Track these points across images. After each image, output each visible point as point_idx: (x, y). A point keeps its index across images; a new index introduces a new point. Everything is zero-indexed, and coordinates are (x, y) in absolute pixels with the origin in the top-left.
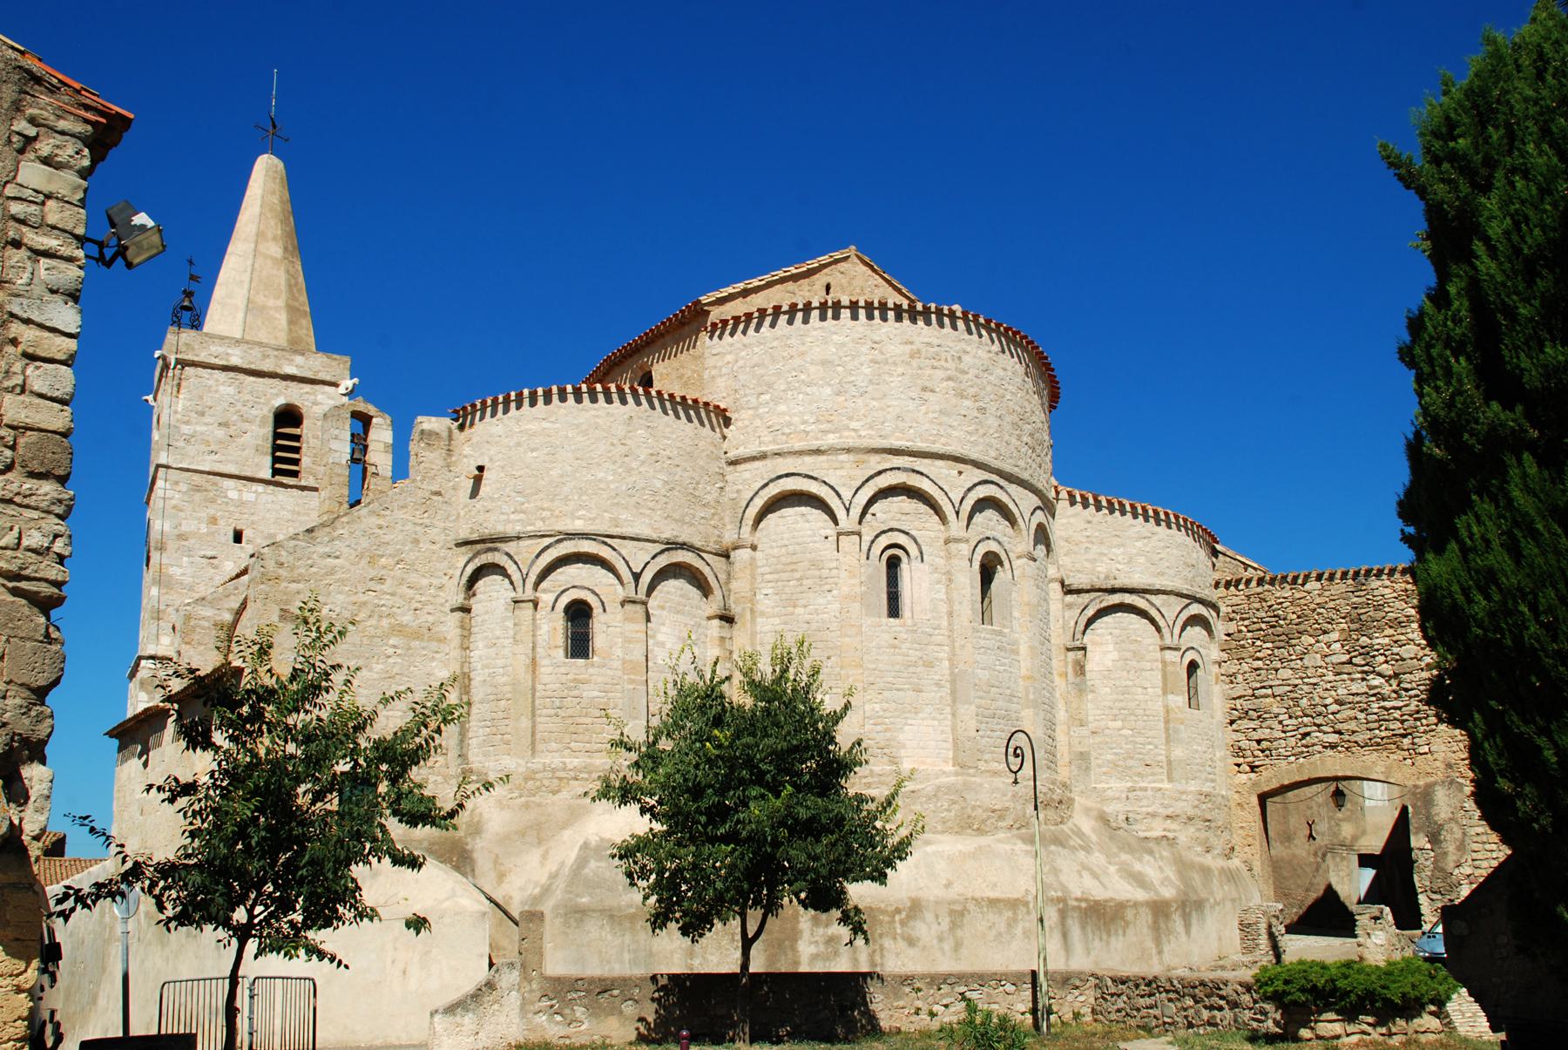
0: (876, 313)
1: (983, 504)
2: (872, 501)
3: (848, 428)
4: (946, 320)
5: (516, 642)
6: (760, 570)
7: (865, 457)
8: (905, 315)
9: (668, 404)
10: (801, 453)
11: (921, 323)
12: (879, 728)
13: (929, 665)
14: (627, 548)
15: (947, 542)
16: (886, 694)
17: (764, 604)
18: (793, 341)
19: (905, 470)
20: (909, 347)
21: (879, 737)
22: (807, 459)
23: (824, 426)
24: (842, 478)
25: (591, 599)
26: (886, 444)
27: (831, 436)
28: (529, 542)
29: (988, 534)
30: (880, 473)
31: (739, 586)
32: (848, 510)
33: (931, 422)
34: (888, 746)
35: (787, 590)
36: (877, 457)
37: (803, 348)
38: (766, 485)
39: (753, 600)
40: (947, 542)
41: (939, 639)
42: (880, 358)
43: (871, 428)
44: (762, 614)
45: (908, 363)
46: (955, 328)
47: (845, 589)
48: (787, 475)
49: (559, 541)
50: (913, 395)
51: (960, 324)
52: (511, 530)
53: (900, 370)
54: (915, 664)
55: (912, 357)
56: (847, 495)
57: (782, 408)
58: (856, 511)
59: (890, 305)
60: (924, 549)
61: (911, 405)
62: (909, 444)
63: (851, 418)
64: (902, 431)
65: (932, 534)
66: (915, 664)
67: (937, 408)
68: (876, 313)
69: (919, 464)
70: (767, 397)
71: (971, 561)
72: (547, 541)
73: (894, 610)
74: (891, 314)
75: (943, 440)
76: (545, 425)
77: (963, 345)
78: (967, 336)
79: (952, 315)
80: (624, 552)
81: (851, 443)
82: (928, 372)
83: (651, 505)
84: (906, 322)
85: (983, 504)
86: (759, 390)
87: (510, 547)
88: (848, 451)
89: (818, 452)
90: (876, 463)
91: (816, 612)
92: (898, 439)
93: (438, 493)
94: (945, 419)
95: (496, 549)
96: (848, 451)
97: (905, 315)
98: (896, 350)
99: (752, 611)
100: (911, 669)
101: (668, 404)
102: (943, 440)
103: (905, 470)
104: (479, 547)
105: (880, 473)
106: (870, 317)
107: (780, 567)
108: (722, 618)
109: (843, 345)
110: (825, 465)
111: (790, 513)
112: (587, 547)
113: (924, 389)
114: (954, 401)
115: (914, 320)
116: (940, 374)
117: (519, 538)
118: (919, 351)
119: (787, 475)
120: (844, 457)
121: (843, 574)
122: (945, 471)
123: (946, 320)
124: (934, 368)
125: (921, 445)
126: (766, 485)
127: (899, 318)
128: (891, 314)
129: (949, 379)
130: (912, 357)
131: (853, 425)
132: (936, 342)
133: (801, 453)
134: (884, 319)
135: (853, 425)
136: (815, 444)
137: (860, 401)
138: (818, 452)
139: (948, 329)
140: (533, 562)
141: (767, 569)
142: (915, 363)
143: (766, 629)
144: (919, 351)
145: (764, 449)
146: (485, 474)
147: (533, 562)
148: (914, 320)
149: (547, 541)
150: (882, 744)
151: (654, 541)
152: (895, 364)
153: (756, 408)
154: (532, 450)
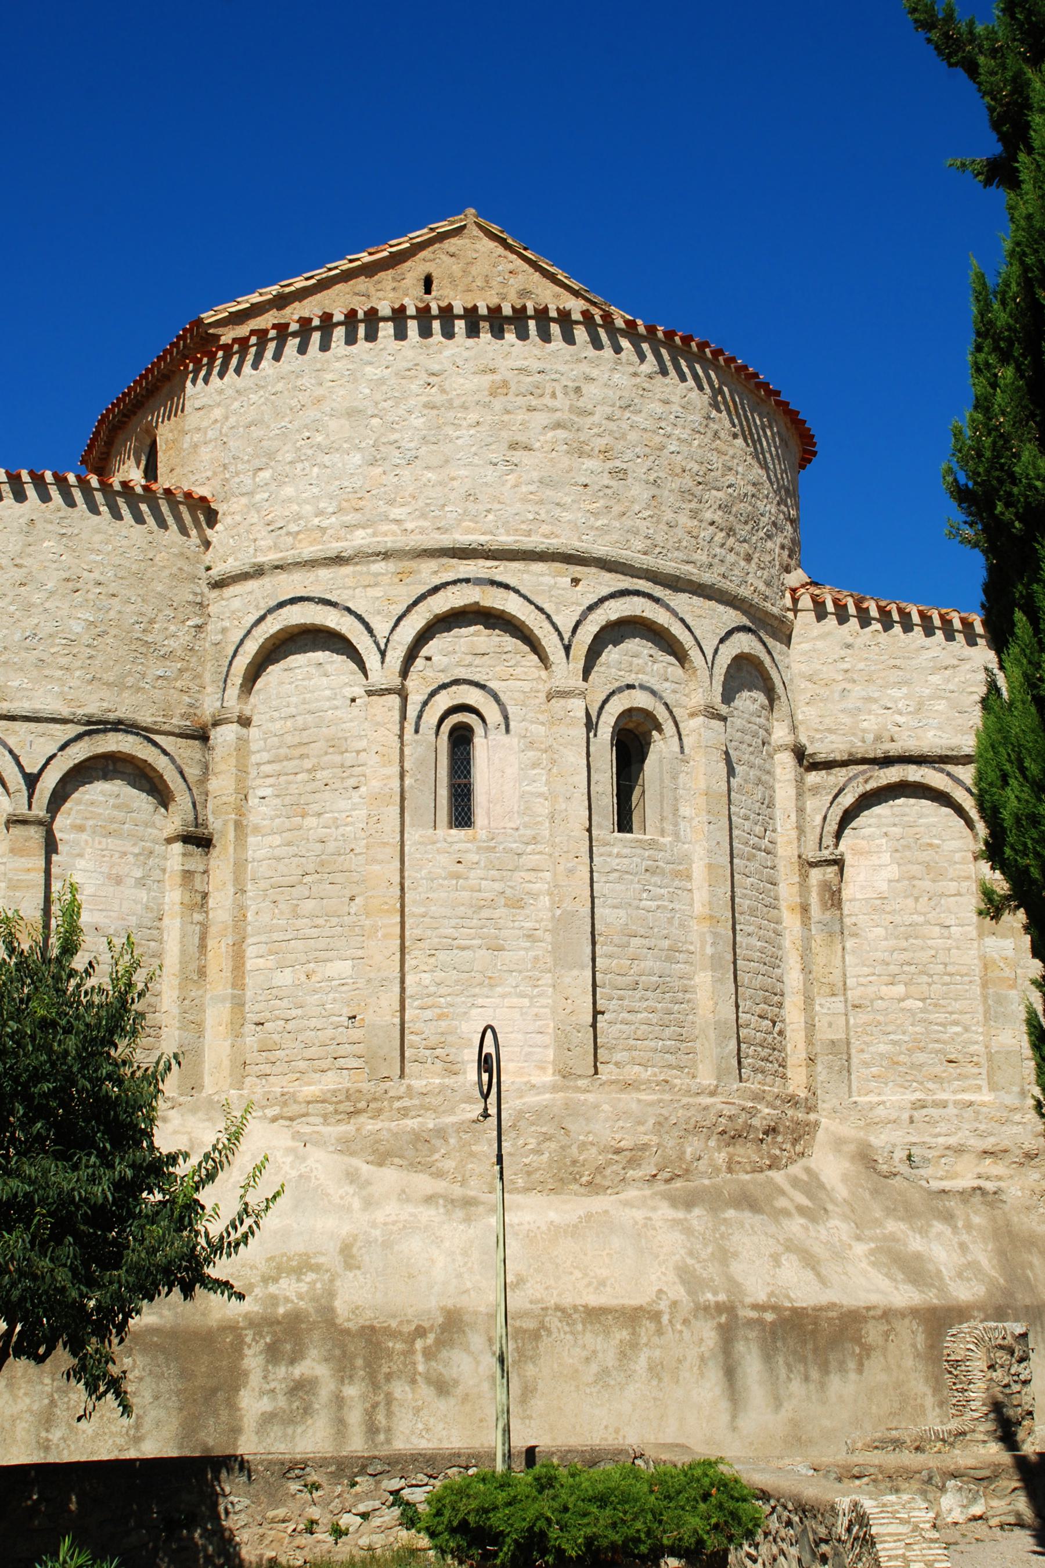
0: (436, 325)
1: (615, 632)
2: (424, 637)
3: (386, 519)
4: (555, 329)
6: (254, 759)
7: (413, 564)
8: (484, 325)
11: (510, 337)
12: (428, 1014)
13: (516, 904)
15: (549, 697)
16: (442, 956)
17: (259, 812)
19: (479, 582)
20: (490, 377)
21: (429, 1030)
22: (323, 573)
23: (350, 518)
24: (378, 602)
26: (446, 541)
30: (436, 589)
31: (221, 784)
33: (525, 500)
34: (442, 1045)
35: (293, 789)
36: (432, 564)
39: (240, 811)
40: (549, 697)
41: (532, 860)
42: (439, 399)
43: (423, 516)
44: (257, 829)
45: (487, 405)
46: (569, 339)
47: (375, 784)
50: (493, 457)
51: (580, 333)
53: (473, 417)
54: (492, 904)
55: (493, 394)
59: (458, 310)
60: (510, 710)
61: (491, 474)
62: (483, 539)
63: (391, 502)
64: (474, 519)
65: (527, 686)
66: (492, 904)
67: (535, 475)
68: (436, 325)
69: (503, 571)
71: (591, 725)
73: (461, 810)
74: (460, 325)
75: (545, 528)
77: (584, 368)
78: (591, 352)
81: (389, 542)
82: (521, 416)
83: (64, 661)
84: (486, 336)
85: (615, 632)
88: (386, 555)
90: (430, 573)
91: (336, 824)
92: (468, 531)
94: (549, 493)
96: (386, 555)
97: (484, 325)
98: (467, 384)
99: (238, 825)
100: (485, 913)
102: (545, 528)
103: (479, 582)
105: (436, 589)
106: (425, 332)
107: (283, 751)
108: (187, 839)
109: (382, 381)
110: (349, 582)
111: (301, 663)
113: (513, 446)
114: (565, 462)
115: (498, 333)
116: (541, 419)
118: (505, 384)
120: (379, 566)
121: (373, 760)
122: (548, 580)
123: (555, 329)
124: (531, 409)
125: (506, 540)
127: (473, 331)
128: (460, 325)
129: (558, 425)
130: (493, 394)
131: (396, 512)
132: (536, 365)
134: (448, 334)
135: (396, 512)
136: (334, 547)
137: (406, 473)
139: (558, 343)
141: (265, 756)
142: (498, 404)
143: (261, 854)
144: (505, 384)
148: (498, 333)
150: (433, 1041)
151: (64, 721)
152: (464, 407)
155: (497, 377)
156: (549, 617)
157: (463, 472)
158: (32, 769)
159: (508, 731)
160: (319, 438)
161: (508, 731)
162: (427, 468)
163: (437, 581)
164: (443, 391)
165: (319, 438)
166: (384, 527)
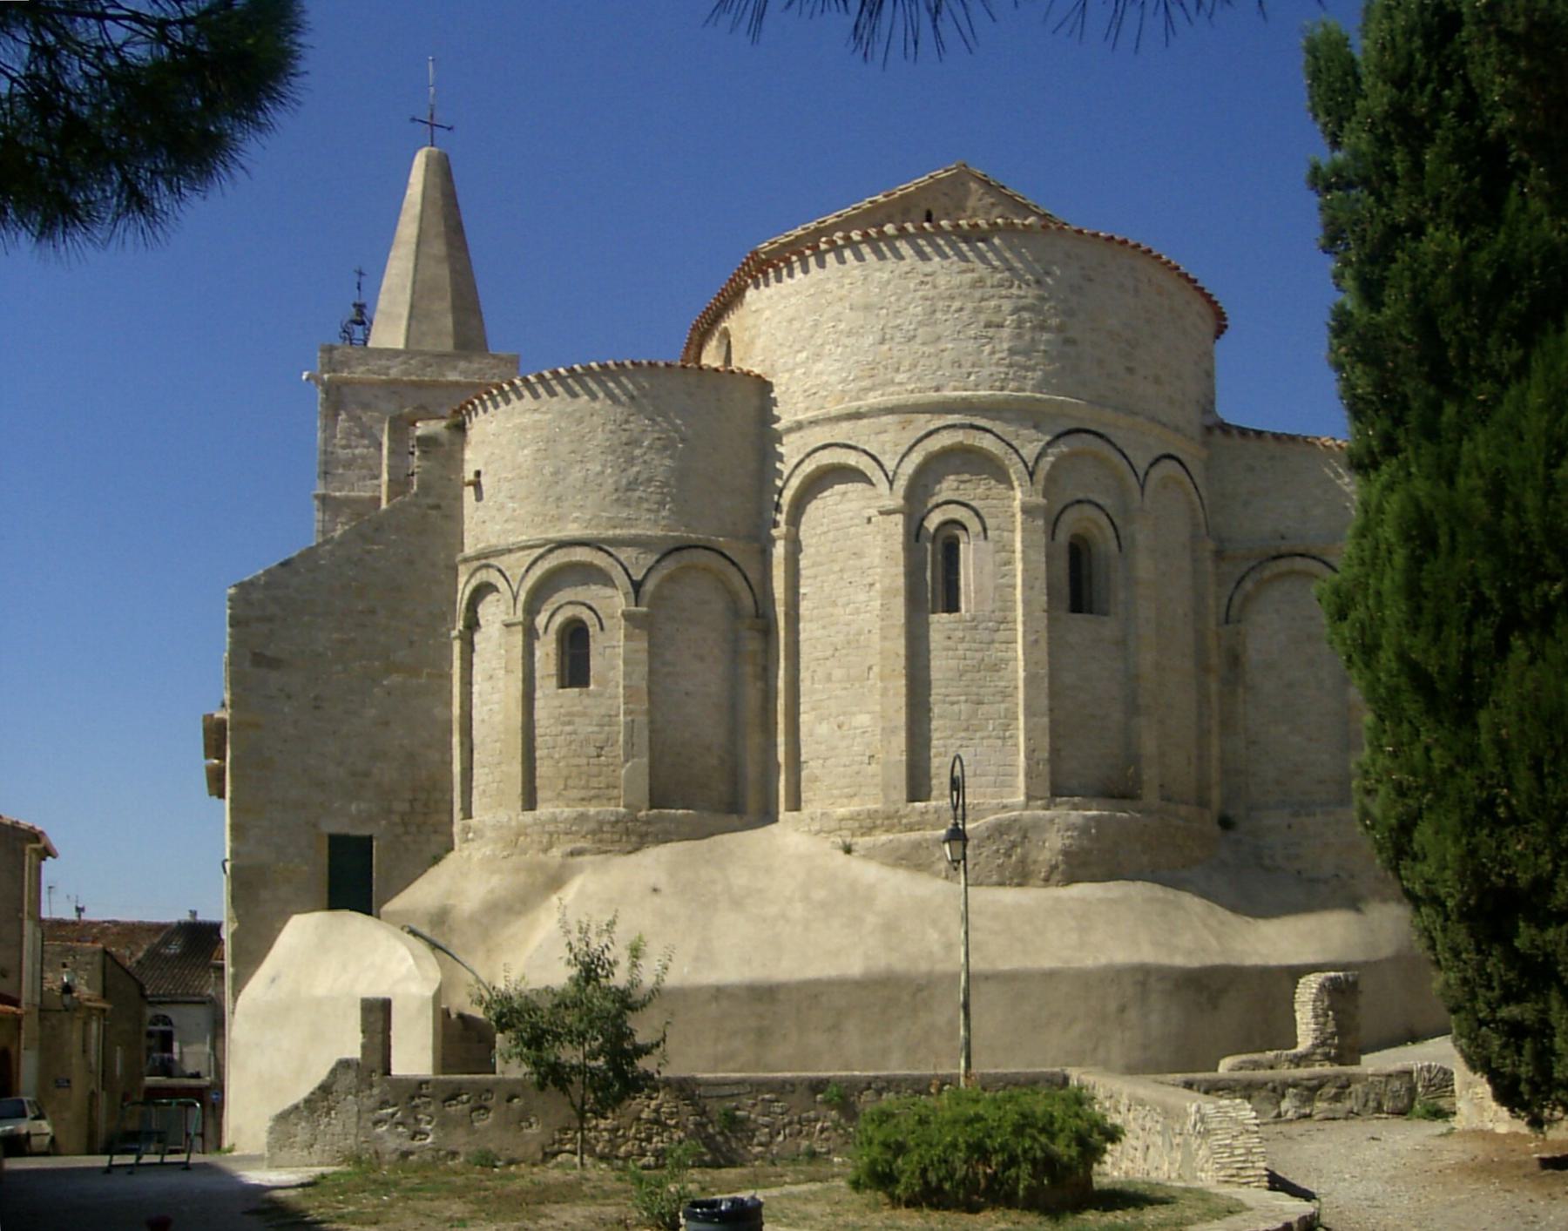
3: (892, 382)
5: (507, 671)
9: (553, 383)
10: (839, 419)
14: (625, 554)
18: (831, 286)
20: (970, 275)
22: (845, 425)
23: (864, 384)
25: (585, 615)
27: (871, 394)
28: (521, 554)
29: (1081, 496)
32: (891, 483)
37: (844, 292)
38: (802, 461)
42: (932, 293)
48: (824, 447)
49: (551, 551)
52: (502, 543)
53: (956, 304)
56: (890, 465)
57: (820, 366)
58: (901, 483)
70: (804, 354)
72: (541, 550)
76: (537, 416)
79: (889, 240)
80: (622, 558)
86: (797, 347)
87: (503, 562)
89: (857, 416)
93: (437, 507)
95: (488, 566)
101: (553, 383)
103: (963, 426)
104: (476, 564)
105: (929, 434)
112: (581, 555)
113: (988, 325)
117: (510, 551)
119: (824, 447)
126: (802, 461)
133: (839, 419)
135: (900, 378)
138: (857, 416)
140: (523, 578)
142: (978, 294)
145: (800, 417)
146: (483, 480)
147: (523, 578)
149: (541, 550)
153: (792, 370)
154: (523, 448)
155: (975, 275)
156: (1017, 451)
157: (950, 346)
158: (637, 577)
159: (986, 538)
160: (842, 326)
161: (986, 538)
162: (924, 344)
163: (931, 427)
164: (935, 287)
165: (842, 326)
166: (892, 389)
